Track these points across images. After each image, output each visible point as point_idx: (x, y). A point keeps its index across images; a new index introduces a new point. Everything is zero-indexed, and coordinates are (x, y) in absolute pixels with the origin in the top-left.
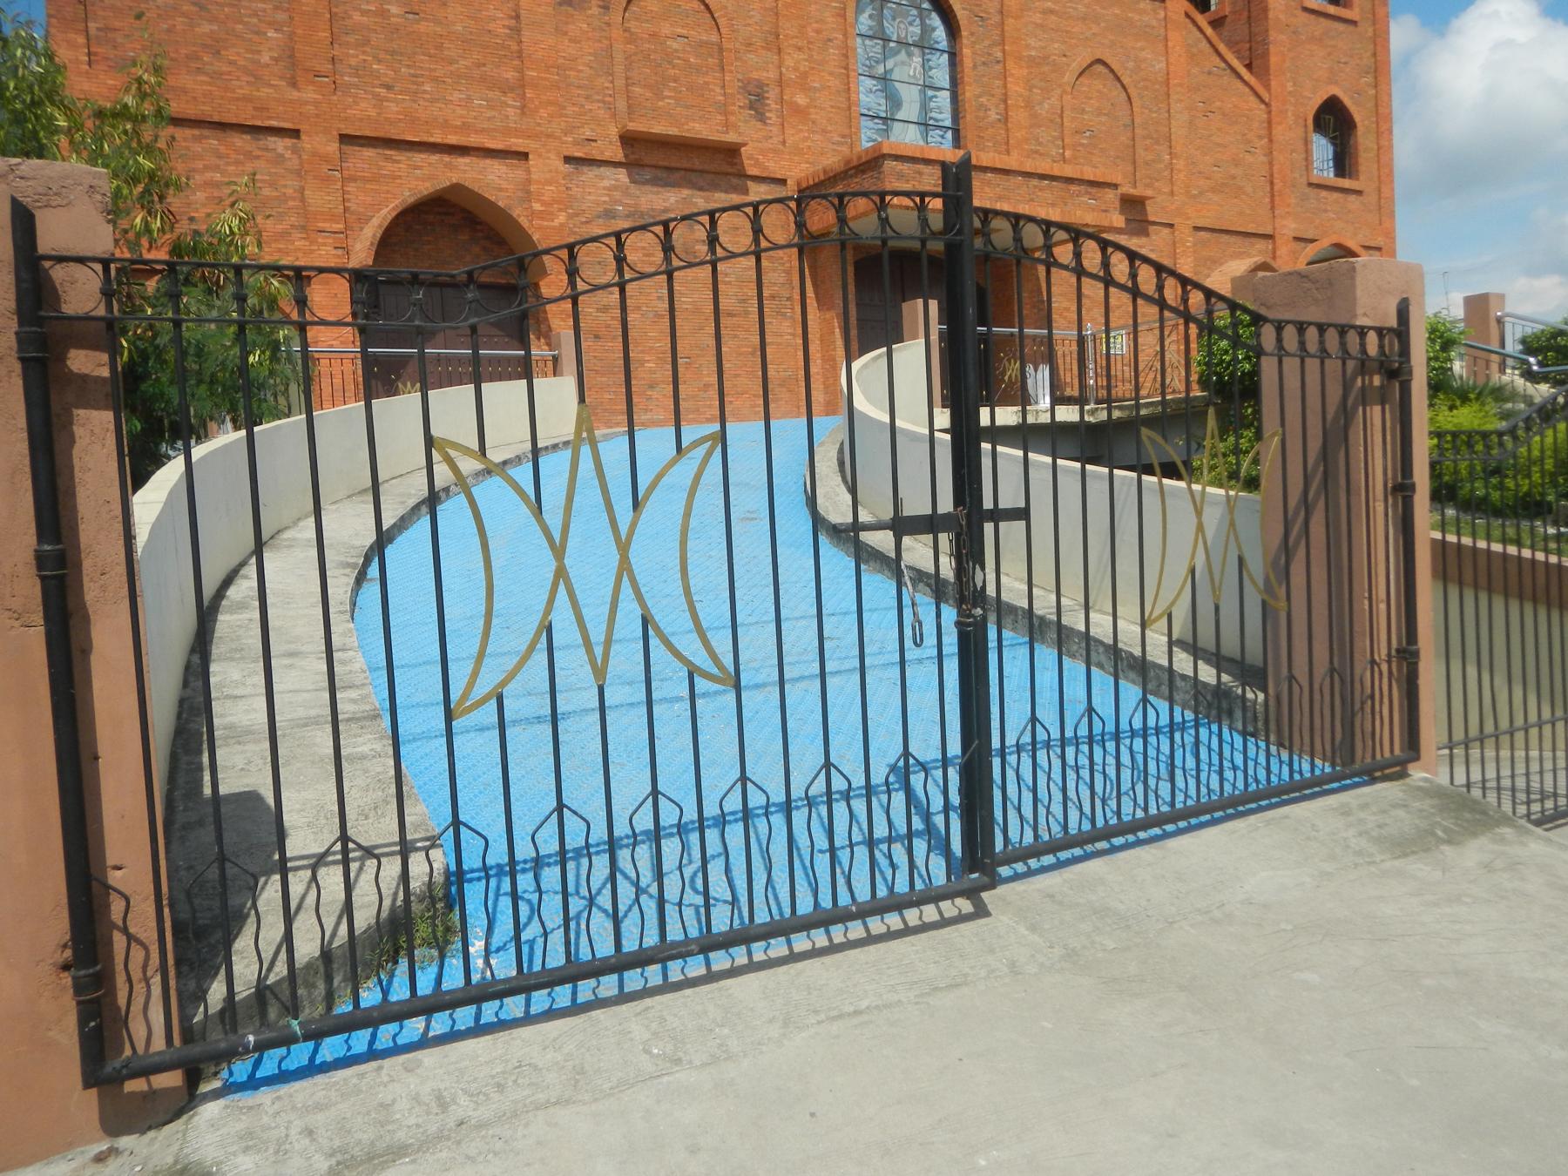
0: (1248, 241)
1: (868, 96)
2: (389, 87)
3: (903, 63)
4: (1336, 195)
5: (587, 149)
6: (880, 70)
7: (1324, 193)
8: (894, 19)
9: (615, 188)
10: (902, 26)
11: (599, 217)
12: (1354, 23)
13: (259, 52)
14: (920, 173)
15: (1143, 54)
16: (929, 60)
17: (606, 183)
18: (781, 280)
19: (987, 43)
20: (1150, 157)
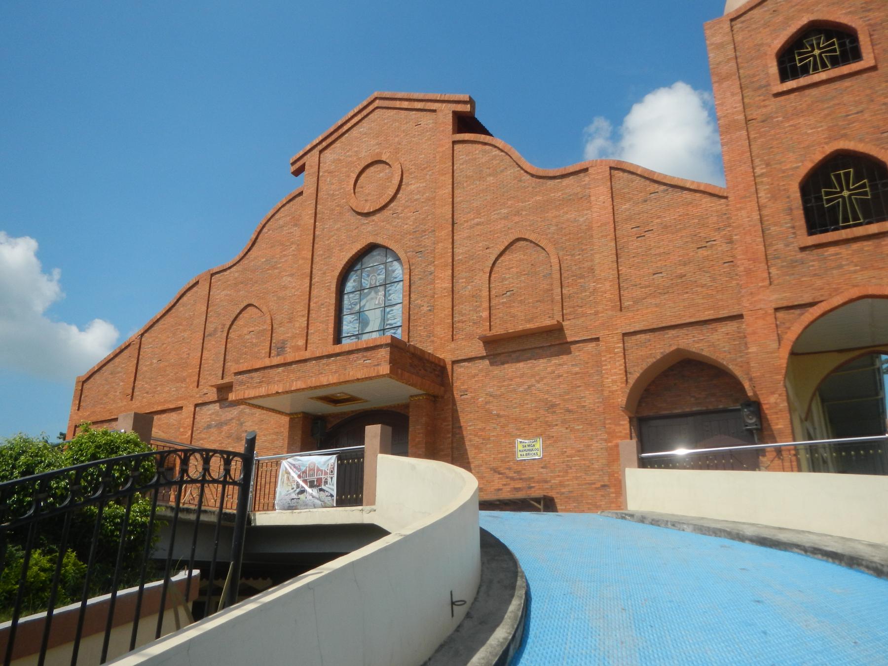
0: (705, 329)
1: (349, 325)
2: (147, 393)
3: (372, 299)
4: (855, 246)
5: (202, 399)
6: (357, 308)
7: (832, 250)
8: (368, 276)
9: (213, 414)
10: (373, 278)
11: (204, 429)
12: (874, 68)
13: (116, 392)
14: (252, 378)
15: (568, 216)
16: (389, 291)
17: (210, 412)
18: (281, 444)
19: (424, 265)
20: (571, 292)
